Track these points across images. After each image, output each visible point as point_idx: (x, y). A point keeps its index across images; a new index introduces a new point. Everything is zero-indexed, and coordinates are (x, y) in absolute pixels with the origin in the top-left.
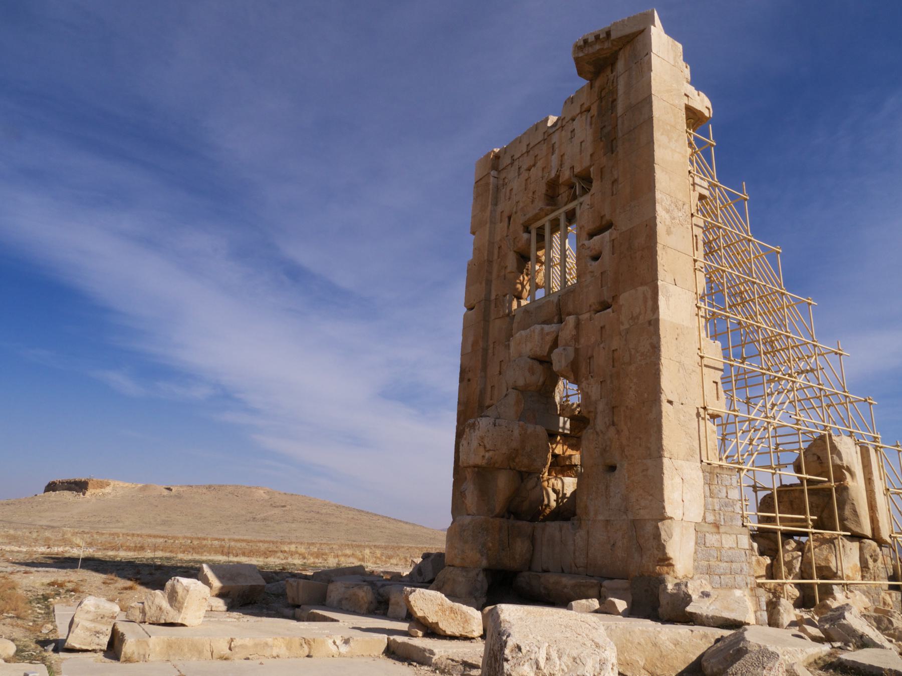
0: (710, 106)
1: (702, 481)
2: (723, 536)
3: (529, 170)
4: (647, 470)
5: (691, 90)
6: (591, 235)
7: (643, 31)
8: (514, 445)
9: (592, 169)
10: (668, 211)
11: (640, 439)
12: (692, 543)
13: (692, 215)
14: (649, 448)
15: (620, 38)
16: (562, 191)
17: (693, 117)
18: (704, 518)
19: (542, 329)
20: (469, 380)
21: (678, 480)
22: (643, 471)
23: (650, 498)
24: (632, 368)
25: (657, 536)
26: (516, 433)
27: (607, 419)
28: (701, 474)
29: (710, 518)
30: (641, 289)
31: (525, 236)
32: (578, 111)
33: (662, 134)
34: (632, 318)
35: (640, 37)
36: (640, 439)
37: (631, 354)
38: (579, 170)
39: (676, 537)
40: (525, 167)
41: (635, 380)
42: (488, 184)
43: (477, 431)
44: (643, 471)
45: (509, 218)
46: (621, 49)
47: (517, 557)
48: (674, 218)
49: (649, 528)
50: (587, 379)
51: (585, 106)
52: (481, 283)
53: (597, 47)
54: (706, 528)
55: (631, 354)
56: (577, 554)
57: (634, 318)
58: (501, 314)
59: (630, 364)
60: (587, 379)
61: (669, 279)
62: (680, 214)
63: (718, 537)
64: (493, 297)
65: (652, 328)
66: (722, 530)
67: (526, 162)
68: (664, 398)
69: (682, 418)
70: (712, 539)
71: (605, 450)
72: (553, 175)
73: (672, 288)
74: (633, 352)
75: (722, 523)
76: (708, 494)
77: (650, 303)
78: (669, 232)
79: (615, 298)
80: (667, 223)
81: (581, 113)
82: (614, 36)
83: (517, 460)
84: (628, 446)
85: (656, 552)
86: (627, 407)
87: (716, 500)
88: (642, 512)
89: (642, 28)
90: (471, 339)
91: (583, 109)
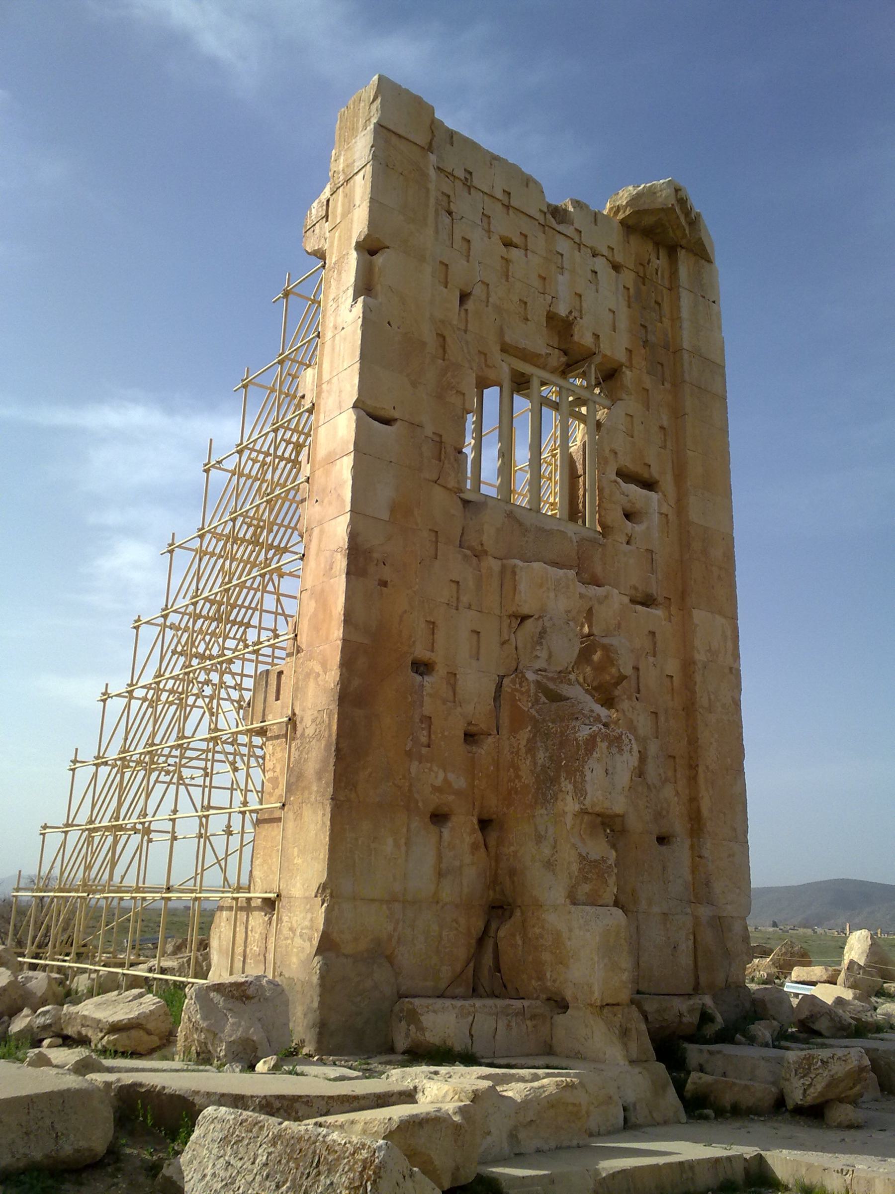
6: (625, 475)
14: (734, 830)
20: (384, 584)
22: (729, 856)
23: (738, 891)
30: (720, 620)
34: (710, 650)
36: (724, 813)
37: (710, 699)
38: (608, 353)
41: (716, 736)
42: (424, 175)
44: (729, 856)
49: (737, 927)
52: (414, 384)
55: (710, 699)
58: (452, 484)
59: (710, 710)
60: (629, 698)
64: (429, 431)
67: (503, 225)
74: (712, 697)
77: (730, 644)
86: (707, 767)
88: (729, 907)
90: (384, 494)
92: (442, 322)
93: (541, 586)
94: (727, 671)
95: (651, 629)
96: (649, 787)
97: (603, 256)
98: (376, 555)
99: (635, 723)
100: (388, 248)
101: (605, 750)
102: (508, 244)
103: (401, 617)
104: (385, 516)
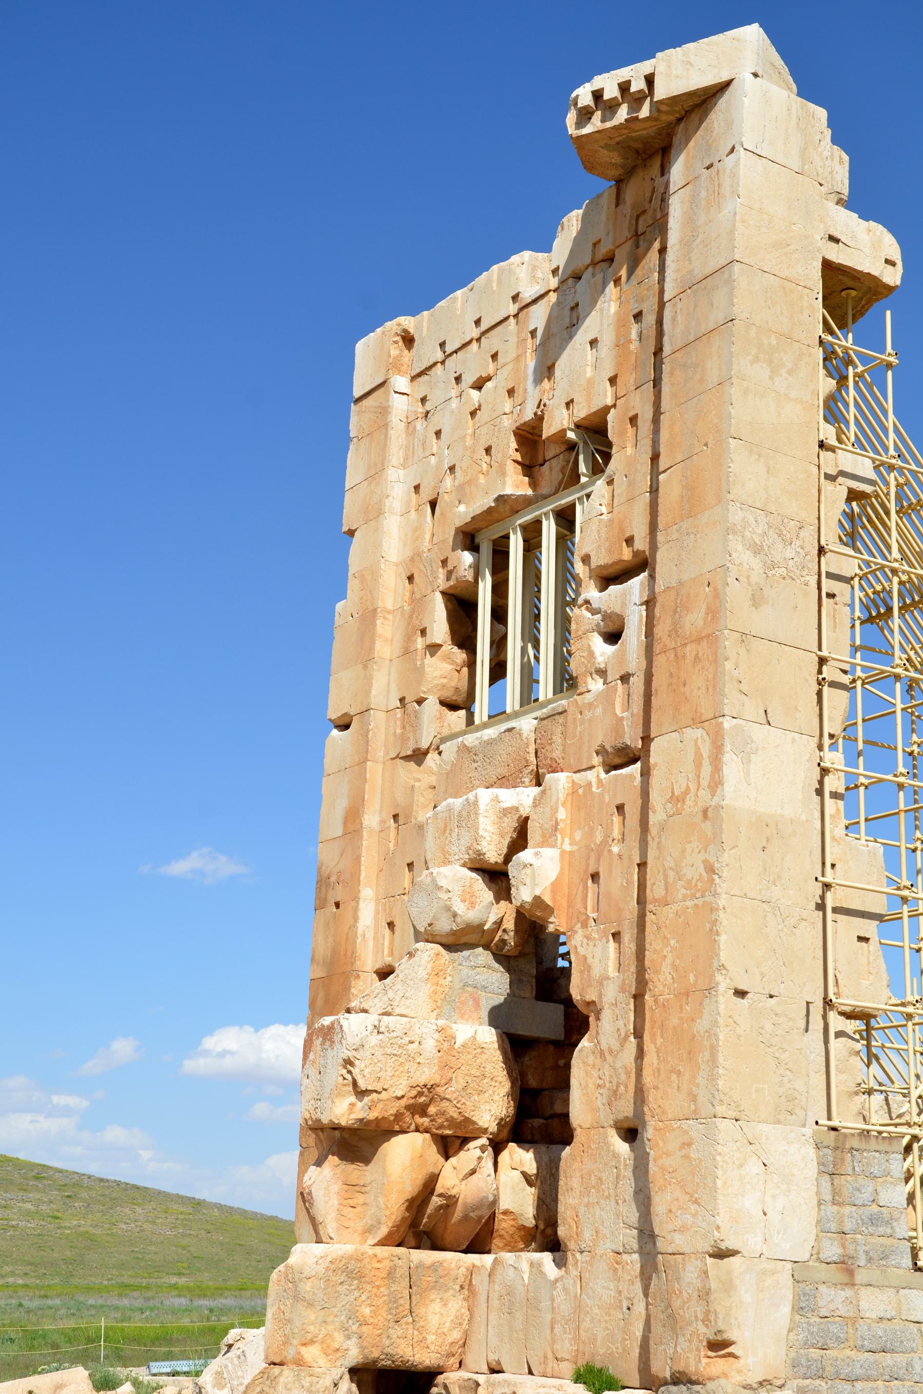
0: (895, 253)
1: (812, 1170)
2: (864, 1292)
3: (478, 386)
4: (690, 1144)
5: (848, 222)
7: (728, 84)
8: (425, 1075)
9: (610, 417)
10: (757, 550)
11: (679, 1073)
12: (786, 1309)
13: (821, 551)
14: (694, 1098)
15: (674, 100)
16: (549, 454)
17: (846, 294)
18: (816, 1254)
19: (496, 800)
21: (754, 1167)
23: (693, 1207)
24: (668, 912)
25: (705, 1295)
26: (430, 1045)
27: (621, 1023)
28: (811, 1152)
29: (832, 1251)
31: (467, 558)
32: (588, 260)
33: (756, 359)
35: (723, 102)
36: (679, 1073)
39: (746, 1293)
40: (469, 379)
41: (673, 942)
42: (384, 411)
43: (337, 1046)
45: (433, 504)
46: (679, 120)
47: (431, 1338)
48: (773, 566)
49: (690, 1274)
50: (585, 925)
51: (603, 250)
52: (365, 667)
53: (623, 114)
54: (822, 1272)
56: (558, 1329)
57: (677, 799)
60: (585, 925)
61: (753, 710)
62: (789, 553)
63: (849, 1292)
65: (707, 827)
66: (861, 1276)
68: (724, 985)
69: (769, 1028)
70: (833, 1299)
71: (615, 1092)
72: (529, 415)
73: (759, 733)
74: (671, 874)
75: (862, 1263)
76: (828, 1197)
77: (706, 769)
78: (757, 601)
79: (647, 739)
80: (754, 579)
81: (594, 264)
82: (661, 92)
83: (432, 1110)
84: (656, 1088)
85: (702, 1329)
87: (847, 1210)
89: (725, 78)
91: (599, 257)
92: (412, 560)
93: (445, 830)
94: (700, 816)
95: (619, 802)
96: (602, 1053)
97: (587, 268)
98: (333, 878)
99: (590, 960)
100: (356, 530)
101: (319, 1048)
102: (478, 386)
103: (348, 934)
104: (339, 832)
